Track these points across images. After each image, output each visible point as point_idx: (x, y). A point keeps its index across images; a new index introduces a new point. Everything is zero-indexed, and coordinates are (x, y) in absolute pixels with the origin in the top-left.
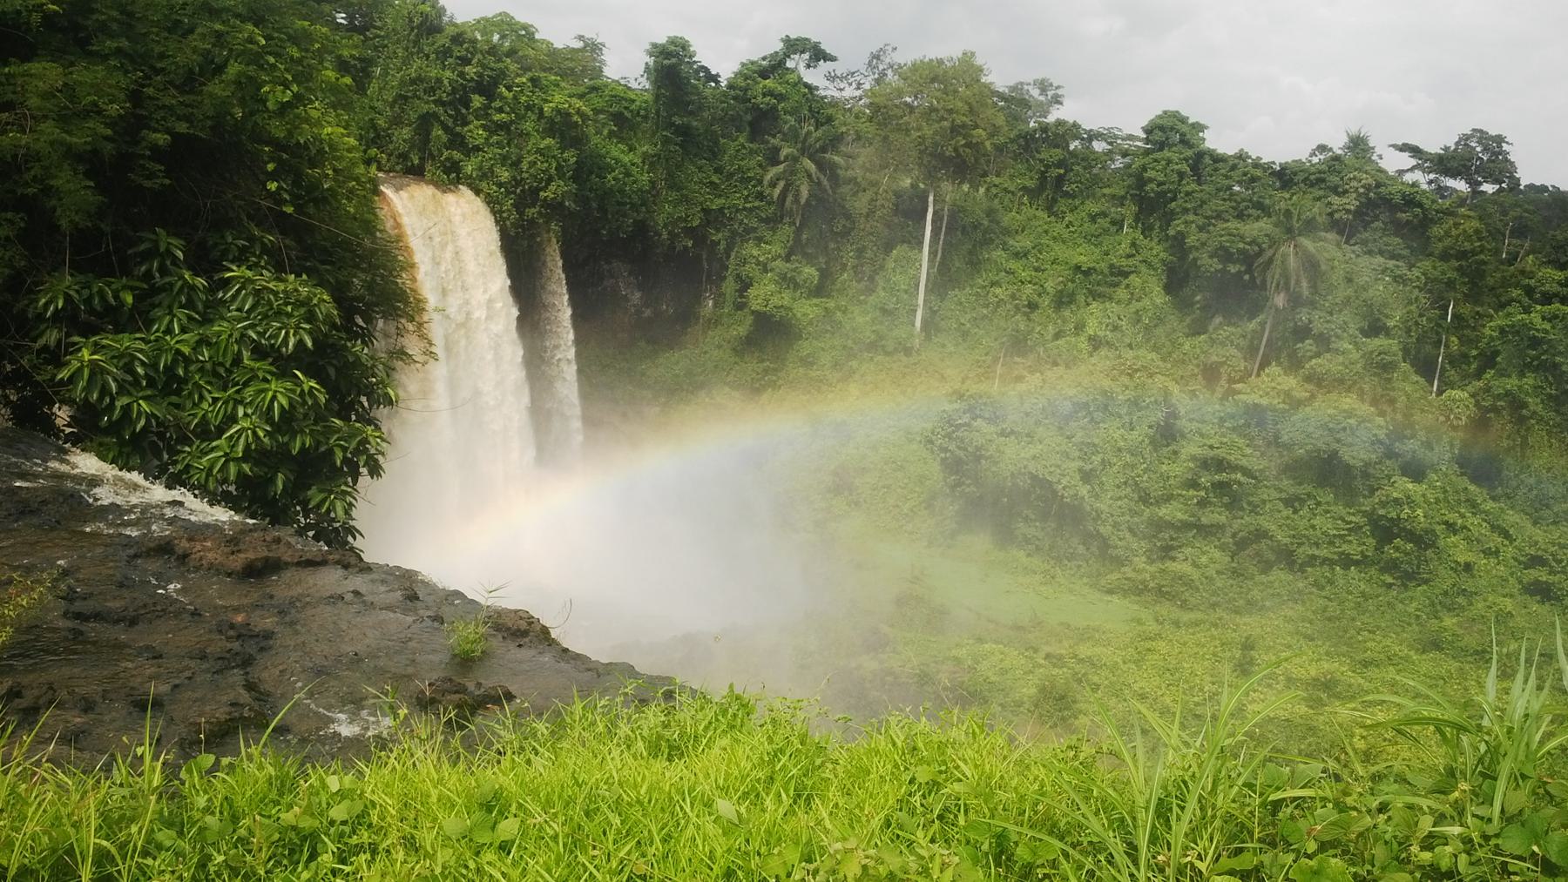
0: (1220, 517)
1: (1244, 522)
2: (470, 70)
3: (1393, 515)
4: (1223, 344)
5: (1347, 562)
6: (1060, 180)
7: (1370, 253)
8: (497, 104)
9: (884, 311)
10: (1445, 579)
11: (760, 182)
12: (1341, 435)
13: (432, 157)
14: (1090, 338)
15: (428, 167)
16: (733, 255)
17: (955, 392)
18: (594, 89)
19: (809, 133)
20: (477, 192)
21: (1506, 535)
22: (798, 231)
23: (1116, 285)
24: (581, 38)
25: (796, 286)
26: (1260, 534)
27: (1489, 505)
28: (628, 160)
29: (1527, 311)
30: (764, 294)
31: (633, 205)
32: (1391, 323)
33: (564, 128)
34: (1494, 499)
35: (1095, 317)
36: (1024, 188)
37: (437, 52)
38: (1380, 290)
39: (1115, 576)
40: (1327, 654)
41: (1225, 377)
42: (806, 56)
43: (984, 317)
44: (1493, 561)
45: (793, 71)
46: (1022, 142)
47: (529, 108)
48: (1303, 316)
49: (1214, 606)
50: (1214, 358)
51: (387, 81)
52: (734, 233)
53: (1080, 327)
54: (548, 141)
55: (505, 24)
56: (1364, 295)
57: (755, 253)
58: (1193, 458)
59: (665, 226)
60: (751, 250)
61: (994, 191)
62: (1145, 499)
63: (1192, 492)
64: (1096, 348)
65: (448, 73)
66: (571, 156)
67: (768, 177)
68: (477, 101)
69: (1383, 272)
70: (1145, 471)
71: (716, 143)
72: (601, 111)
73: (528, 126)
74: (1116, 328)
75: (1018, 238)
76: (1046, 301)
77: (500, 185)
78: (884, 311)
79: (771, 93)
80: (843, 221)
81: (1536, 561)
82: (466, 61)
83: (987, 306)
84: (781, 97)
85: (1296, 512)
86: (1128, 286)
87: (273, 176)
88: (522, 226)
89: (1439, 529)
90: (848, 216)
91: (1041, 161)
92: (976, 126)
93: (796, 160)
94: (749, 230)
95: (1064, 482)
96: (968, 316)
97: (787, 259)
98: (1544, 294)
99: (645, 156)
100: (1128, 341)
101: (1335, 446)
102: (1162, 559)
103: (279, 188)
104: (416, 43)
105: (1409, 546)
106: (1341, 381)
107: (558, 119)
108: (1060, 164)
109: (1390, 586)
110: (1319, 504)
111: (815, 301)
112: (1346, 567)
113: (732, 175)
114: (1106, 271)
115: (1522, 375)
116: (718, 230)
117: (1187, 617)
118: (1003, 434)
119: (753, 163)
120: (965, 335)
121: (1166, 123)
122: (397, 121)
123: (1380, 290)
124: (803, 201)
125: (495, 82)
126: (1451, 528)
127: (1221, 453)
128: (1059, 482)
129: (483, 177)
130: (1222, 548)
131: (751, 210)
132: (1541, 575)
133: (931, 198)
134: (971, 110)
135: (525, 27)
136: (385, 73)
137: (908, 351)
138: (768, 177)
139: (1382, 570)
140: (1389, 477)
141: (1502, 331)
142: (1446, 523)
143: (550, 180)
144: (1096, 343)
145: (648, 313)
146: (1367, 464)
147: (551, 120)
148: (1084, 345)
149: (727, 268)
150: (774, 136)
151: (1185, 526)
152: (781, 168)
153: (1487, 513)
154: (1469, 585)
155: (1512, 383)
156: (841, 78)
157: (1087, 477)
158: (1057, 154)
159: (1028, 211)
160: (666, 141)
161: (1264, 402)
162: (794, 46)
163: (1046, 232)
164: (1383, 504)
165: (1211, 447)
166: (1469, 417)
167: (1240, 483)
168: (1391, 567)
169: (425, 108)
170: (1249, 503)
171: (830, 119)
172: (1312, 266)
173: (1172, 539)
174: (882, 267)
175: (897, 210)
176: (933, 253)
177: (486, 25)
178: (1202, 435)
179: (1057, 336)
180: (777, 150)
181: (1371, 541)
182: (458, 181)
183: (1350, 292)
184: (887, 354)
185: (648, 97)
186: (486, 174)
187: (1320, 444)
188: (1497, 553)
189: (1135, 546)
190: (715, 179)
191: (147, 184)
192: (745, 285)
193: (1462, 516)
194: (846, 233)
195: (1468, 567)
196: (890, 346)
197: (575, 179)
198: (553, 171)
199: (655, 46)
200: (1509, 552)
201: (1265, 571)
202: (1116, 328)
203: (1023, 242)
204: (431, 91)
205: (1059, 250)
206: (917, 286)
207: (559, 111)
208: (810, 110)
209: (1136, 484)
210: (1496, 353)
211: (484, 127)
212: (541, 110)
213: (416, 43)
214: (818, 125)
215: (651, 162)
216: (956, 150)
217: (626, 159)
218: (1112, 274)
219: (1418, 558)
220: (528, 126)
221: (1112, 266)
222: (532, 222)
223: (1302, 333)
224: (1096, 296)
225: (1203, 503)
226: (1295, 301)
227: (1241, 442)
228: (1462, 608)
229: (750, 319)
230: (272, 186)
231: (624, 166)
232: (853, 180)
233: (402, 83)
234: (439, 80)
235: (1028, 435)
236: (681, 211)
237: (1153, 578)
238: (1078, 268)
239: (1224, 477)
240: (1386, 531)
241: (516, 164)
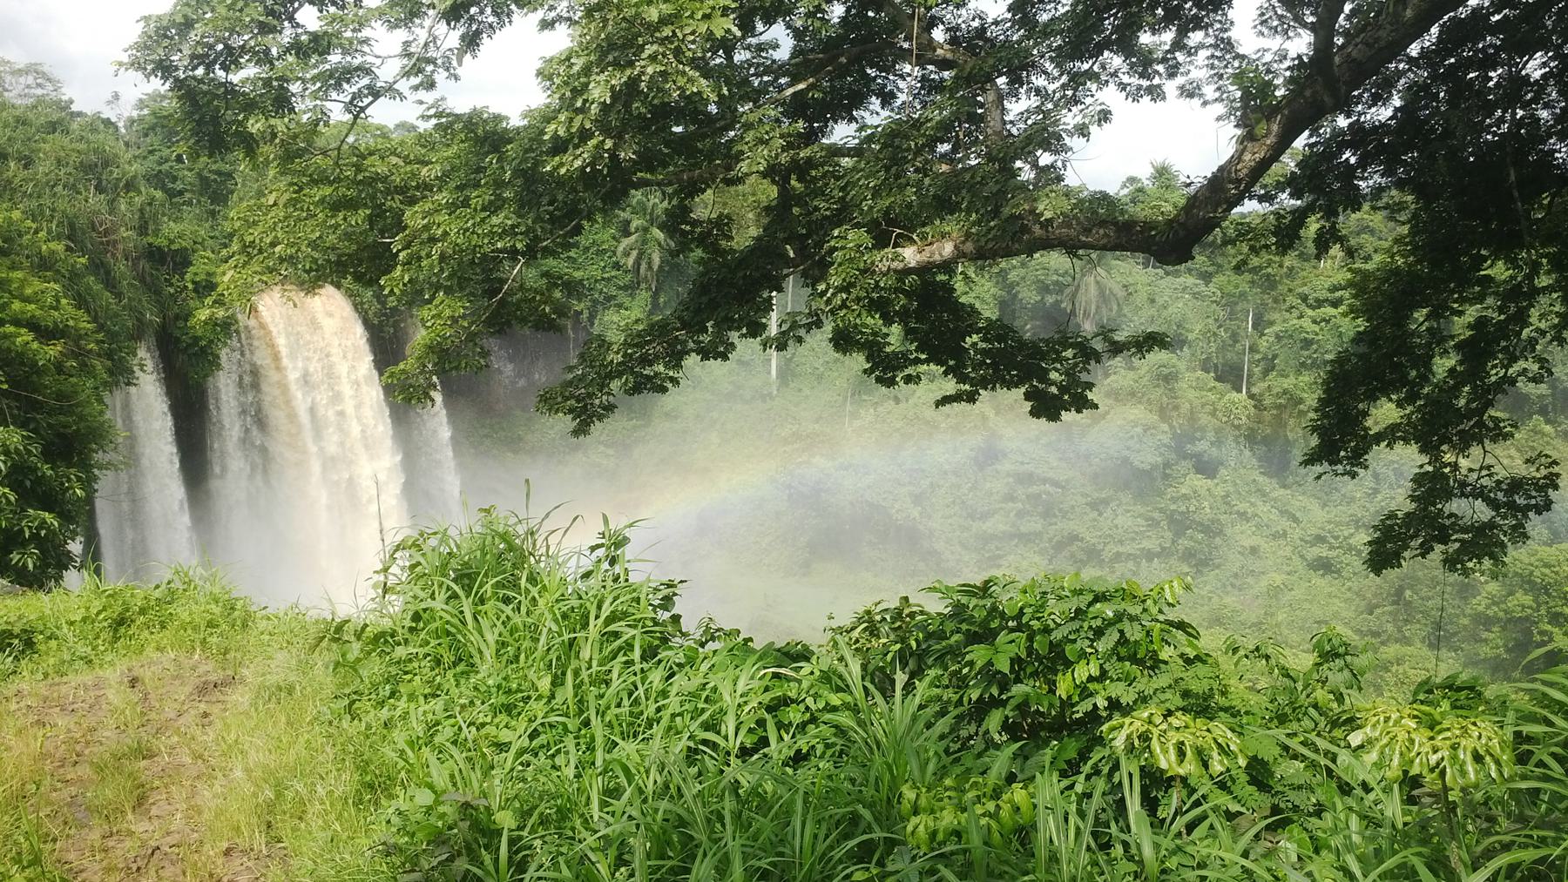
3: (1183, 508)
5: (1150, 556)
11: (614, 253)
20: (338, 286)
21: (1296, 520)
22: (655, 296)
26: (1074, 538)
34: (1285, 487)
57: (615, 319)
58: (1008, 475)
62: (971, 516)
63: (1011, 505)
70: (970, 490)
81: (1320, 539)
85: (1100, 514)
88: (385, 315)
94: (609, 298)
112: (1150, 560)
113: (587, 249)
116: (580, 301)
124: (655, 268)
127: (1029, 468)
130: (1041, 552)
132: (1322, 551)
151: (1012, 536)
152: (633, 237)
153: (1275, 500)
164: (1174, 500)
166: (1248, 417)
167: (1049, 494)
168: (1188, 555)
181: (1169, 535)
188: (1285, 534)
195: (1254, 550)
200: (1296, 534)
219: (1208, 546)
239: (1034, 489)
240: (1180, 524)
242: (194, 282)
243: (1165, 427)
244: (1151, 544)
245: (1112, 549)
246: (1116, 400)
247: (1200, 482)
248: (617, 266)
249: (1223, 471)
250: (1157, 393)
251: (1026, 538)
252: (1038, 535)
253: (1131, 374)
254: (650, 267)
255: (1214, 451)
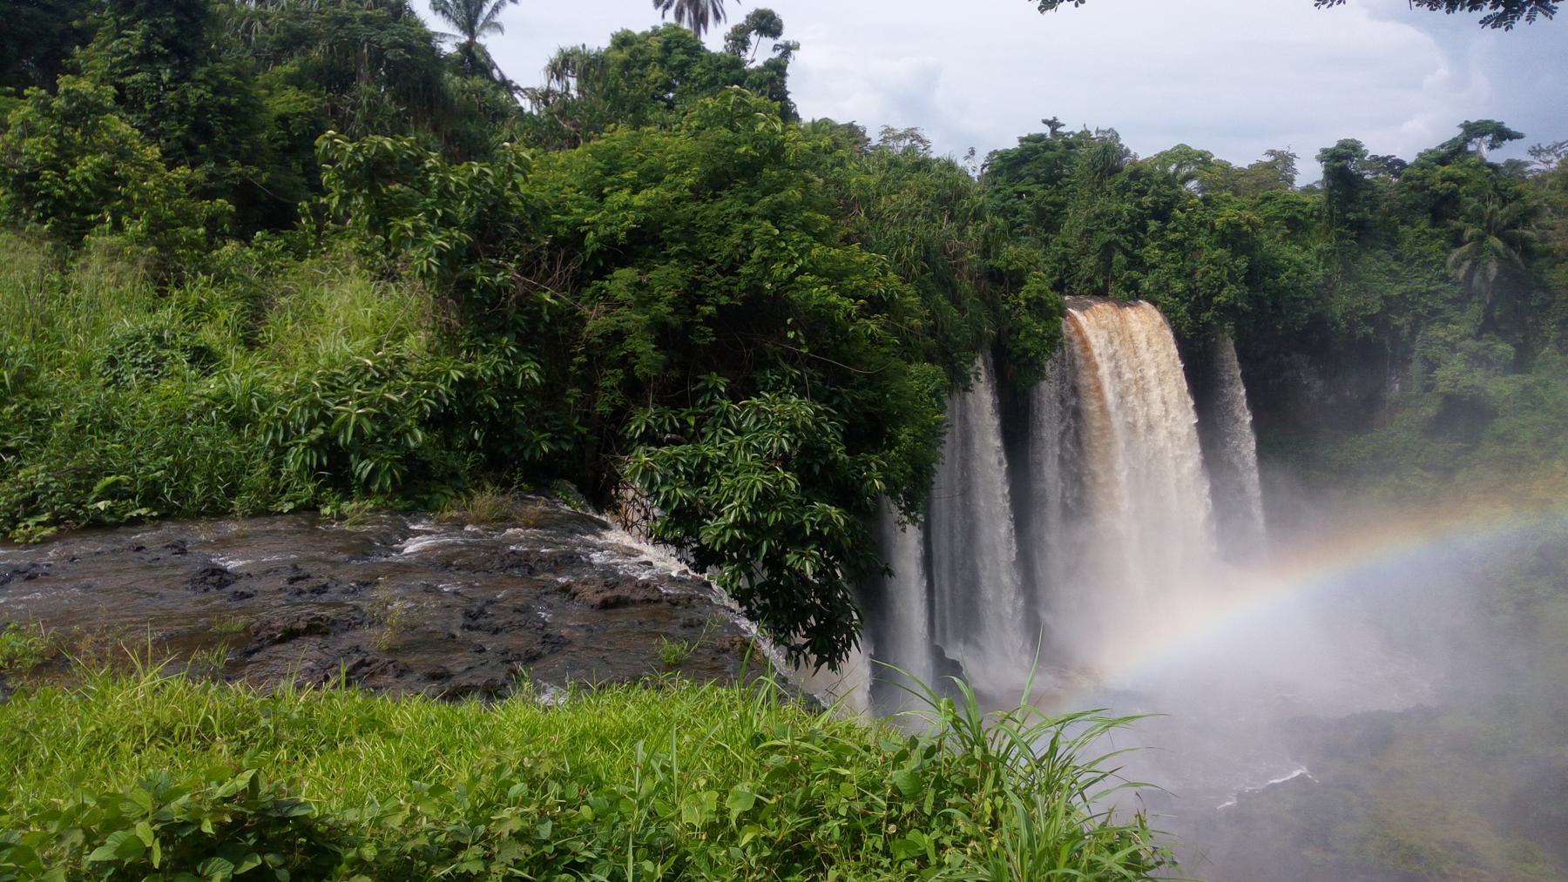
2: (1147, 200)
8: (1171, 225)
11: (1444, 265)
13: (1115, 278)
15: (1111, 286)
16: (1418, 337)
18: (1268, 198)
19: (1493, 212)
24: (1271, 153)
25: (1490, 364)
28: (1303, 260)
30: (1454, 373)
31: (1309, 301)
33: (1235, 238)
37: (1117, 189)
42: (1489, 138)
45: (1473, 153)
47: (1201, 224)
51: (1076, 218)
52: (1418, 317)
54: (1219, 251)
55: (1183, 155)
57: (1441, 334)
59: (1343, 316)
60: (1437, 331)
65: (1127, 206)
66: (1242, 263)
67: (1451, 259)
68: (1153, 225)
71: (1395, 231)
72: (1277, 218)
73: (1201, 240)
77: (1175, 295)
79: (1451, 178)
80: (1542, 295)
82: (1142, 193)
84: (1460, 181)
87: (792, 328)
90: (1546, 288)
93: (1481, 238)
94: (1434, 312)
97: (1478, 337)
99: (1320, 253)
103: (797, 335)
104: (1099, 184)
107: (1229, 231)
111: (1511, 377)
116: (1400, 315)
119: (1433, 248)
122: (1084, 253)
124: (1492, 278)
125: (1170, 206)
129: (1160, 289)
131: (1435, 292)
135: (1201, 154)
136: (1075, 212)
138: (1451, 259)
143: (1223, 285)
145: (1330, 400)
147: (1223, 233)
149: (1412, 351)
150: (1456, 219)
152: (1466, 248)
156: (1549, 151)
160: (1341, 236)
162: (1473, 130)
169: (1107, 238)
171: (1518, 195)
177: (1164, 158)
180: (1460, 232)
182: (1137, 297)
185: (1321, 198)
186: (1162, 287)
190: (1394, 266)
191: (700, 342)
192: (1432, 365)
194: (1545, 307)
197: (1247, 282)
198: (1225, 278)
199: (1325, 151)
204: (1112, 222)
207: (1229, 224)
208: (1496, 188)
211: (1160, 247)
212: (1213, 225)
213: (1099, 184)
214: (1505, 201)
215: (1326, 258)
217: (1299, 258)
220: (1201, 240)
222: (1207, 325)
229: (1438, 401)
230: (791, 335)
231: (1297, 265)
232: (1548, 253)
233: (1088, 219)
234: (1119, 213)
236: (1359, 301)
241: (1190, 275)
242: (1027, 300)
248: (1445, 278)
254: (1485, 278)
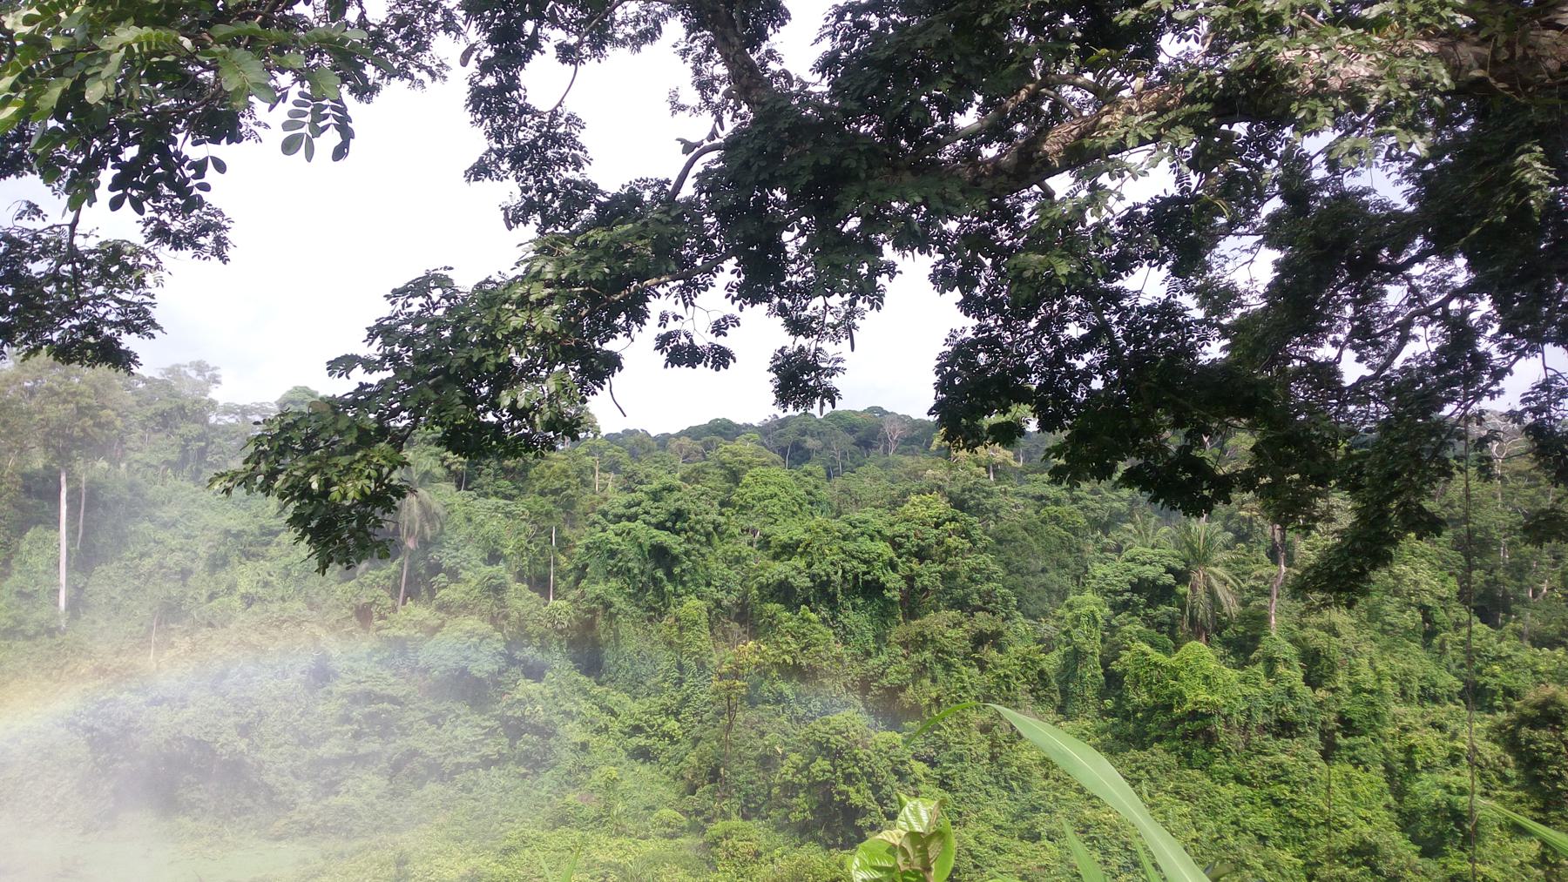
0: (374, 745)
1: (399, 744)
3: (519, 714)
4: (370, 586)
5: (487, 763)
6: (202, 452)
7: (486, 495)
9: (21, 594)
10: (568, 759)
12: (468, 653)
14: (243, 597)
17: (96, 669)
21: (613, 713)
23: (268, 543)
26: (414, 753)
27: (597, 690)
29: (604, 530)
32: (507, 551)
34: (601, 684)
35: (246, 577)
36: (168, 463)
38: (494, 525)
39: (283, 821)
40: (475, 851)
41: (375, 615)
43: (137, 588)
44: (604, 736)
46: (159, 419)
48: (434, 555)
49: (377, 829)
50: (364, 600)
53: (231, 588)
56: (482, 531)
58: (344, 695)
61: (135, 466)
62: (305, 741)
63: (347, 727)
64: (249, 605)
69: (496, 509)
70: (302, 715)
74: (266, 584)
75: (165, 508)
76: (199, 566)
78: (21, 594)
81: (637, 729)
83: (138, 577)
85: (439, 727)
86: (279, 544)
89: (556, 719)
91: (182, 436)
92: (104, 407)
95: (221, 740)
96: (118, 590)
98: (615, 515)
100: (279, 594)
101: (463, 663)
102: (327, 795)
105: (535, 738)
106: (465, 606)
108: (200, 438)
109: (524, 776)
110: (458, 716)
114: (257, 532)
115: (607, 580)
117: (356, 844)
118: (156, 702)
120: (117, 609)
121: (296, 397)
123: (494, 525)
126: (568, 714)
127: (367, 686)
128: (216, 741)
132: (640, 740)
133: (63, 478)
134: (96, 391)
137: (51, 632)
139: (518, 764)
140: (515, 681)
141: (588, 548)
142: (564, 712)
144: (249, 600)
146: (492, 674)
148: (237, 602)
151: (349, 759)
153: (594, 697)
154: (587, 761)
155: (599, 588)
157: (244, 730)
158: (194, 429)
159: (172, 482)
161: (403, 633)
163: (194, 501)
164: (510, 706)
165: (359, 682)
168: (524, 759)
170: (399, 728)
172: (428, 514)
173: (334, 774)
174: (17, 551)
175: (27, 490)
176: (72, 532)
178: (354, 672)
179: (212, 597)
181: (506, 740)
183: (470, 529)
184: (29, 638)
187: (451, 664)
188: (607, 728)
189: (300, 788)
193: (577, 703)
195: (584, 746)
196: (31, 629)
200: (616, 726)
201: (420, 787)
202: (266, 584)
203: (170, 512)
205: (208, 517)
206: (58, 565)
209: (295, 729)
210: (586, 566)
216: (83, 430)
218: (263, 534)
221: (262, 527)
223: (436, 569)
224: (248, 556)
225: (357, 735)
226: (425, 544)
227: (387, 673)
228: (584, 783)
235: (181, 699)
237: (318, 816)
238: (227, 532)
239: (373, 708)
240: (515, 729)
243: (498, 635)
244: (490, 750)
245: (452, 760)
246: (448, 613)
247: (531, 687)
249: (549, 674)
250: (487, 604)
251: (363, 761)
252: (376, 755)
253: (462, 587)
255: (539, 657)
